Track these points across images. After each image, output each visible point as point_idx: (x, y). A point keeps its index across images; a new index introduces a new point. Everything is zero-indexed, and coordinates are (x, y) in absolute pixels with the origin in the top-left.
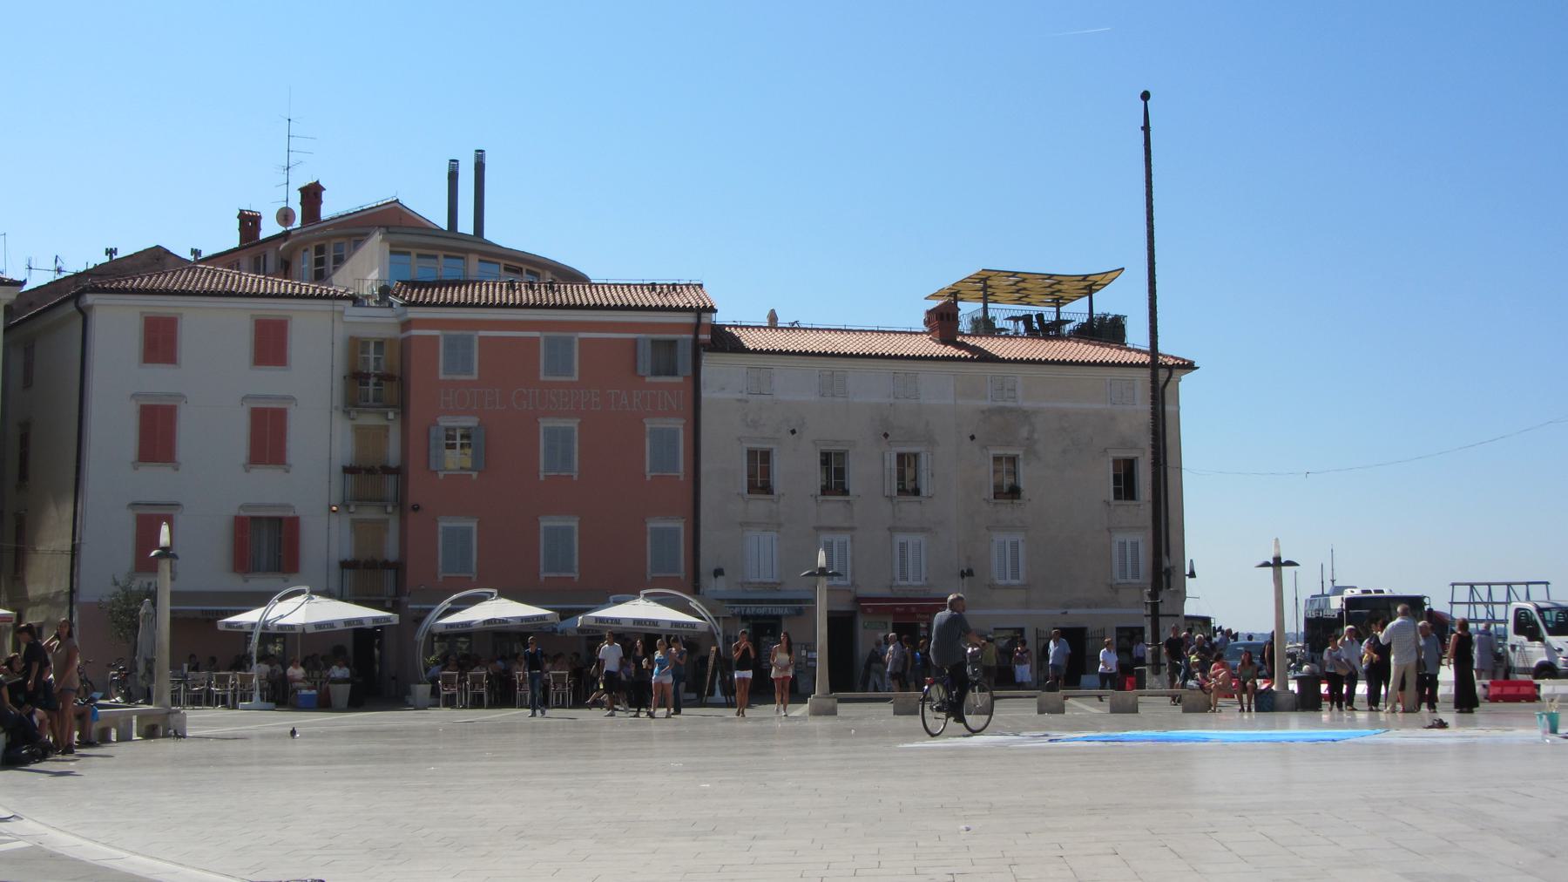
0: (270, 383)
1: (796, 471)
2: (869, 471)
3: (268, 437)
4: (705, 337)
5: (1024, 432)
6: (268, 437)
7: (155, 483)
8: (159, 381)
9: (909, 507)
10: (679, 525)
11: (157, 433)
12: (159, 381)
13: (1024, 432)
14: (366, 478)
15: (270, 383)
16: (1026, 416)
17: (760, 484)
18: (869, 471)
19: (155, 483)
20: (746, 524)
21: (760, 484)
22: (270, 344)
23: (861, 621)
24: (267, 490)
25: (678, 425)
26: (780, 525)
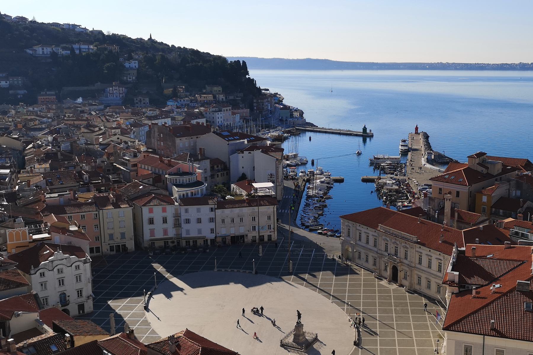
0: (165, 214)
3: (165, 221)
6: (165, 221)
7: (151, 227)
11: (151, 221)
12: (151, 215)
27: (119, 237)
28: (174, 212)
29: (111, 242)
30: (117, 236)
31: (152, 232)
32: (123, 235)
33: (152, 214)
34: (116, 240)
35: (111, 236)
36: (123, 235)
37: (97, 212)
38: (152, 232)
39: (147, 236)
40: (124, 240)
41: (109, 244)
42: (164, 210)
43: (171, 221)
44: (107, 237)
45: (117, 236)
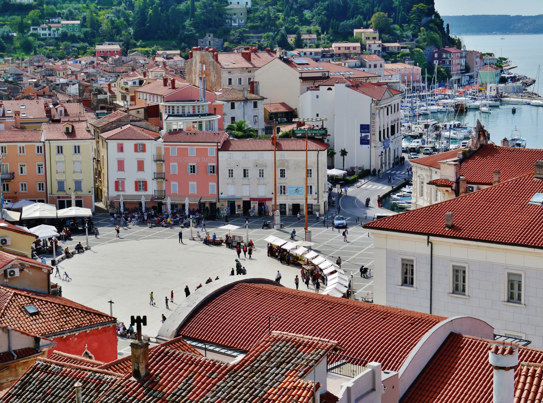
2: (253, 173)
3: (141, 166)
4: (219, 147)
5: (287, 164)
6: (141, 166)
8: (121, 155)
9: (262, 180)
10: (215, 184)
11: (121, 166)
12: (121, 155)
13: (287, 164)
15: (140, 156)
16: (287, 161)
19: (121, 175)
20: (228, 184)
23: (251, 202)
24: (141, 176)
26: (235, 184)
27: (73, 187)
28: (154, 152)
29: (61, 194)
32: (78, 185)
33: (121, 153)
34: (68, 191)
35: (61, 184)
37: (42, 144)
40: (79, 193)
41: (59, 197)
43: (151, 168)
44: (55, 187)
45: (70, 185)
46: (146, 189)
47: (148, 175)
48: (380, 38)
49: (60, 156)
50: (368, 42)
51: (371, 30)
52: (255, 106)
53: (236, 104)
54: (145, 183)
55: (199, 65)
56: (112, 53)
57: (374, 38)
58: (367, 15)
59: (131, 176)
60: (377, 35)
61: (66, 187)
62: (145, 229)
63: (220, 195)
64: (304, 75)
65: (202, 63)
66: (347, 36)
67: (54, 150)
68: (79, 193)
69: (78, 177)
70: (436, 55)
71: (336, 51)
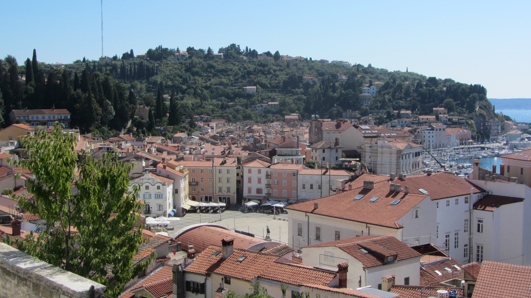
0: (259, 175)
1: (308, 186)
2: (316, 187)
3: (259, 181)
6: (259, 181)
8: (250, 175)
11: (250, 180)
12: (250, 175)
14: (268, 186)
15: (259, 175)
17: (304, 188)
18: (316, 187)
19: (250, 185)
21: (304, 188)
22: (259, 172)
25: (296, 181)
27: (226, 191)
29: (220, 194)
30: (224, 189)
31: (250, 190)
32: (229, 189)
34: (224, 193)
35: (220, 189)
36: (229, 189)
38: (250, 190)
39: (245, 193)
40: (229, 194)
42: (259, 172)
43: (264, 181)
44: (218, 190)
45: (224, 189)
46: (261, 193)
47: (263, 186)
48: (448, 113)
49: (220, 174)
50: (440, 116)
51: (443, 109)
52: (337, 152)
53: (326, 150)
54: (261, 190)
55: (314, 128)
56: (294, 120)
57: (445, 113)
58: (442, 100)
59: (255, 185)
60: (446, 111)
61: (223, 191)
62: (262, 214)
63: (299, 198)
64: (366, 135)
65: (316, 127)
66: (430, 112)
67: (218, 171)
68: (229, 194)
69: (228, 185)
70: (482, 124)
71: (421, 121)
